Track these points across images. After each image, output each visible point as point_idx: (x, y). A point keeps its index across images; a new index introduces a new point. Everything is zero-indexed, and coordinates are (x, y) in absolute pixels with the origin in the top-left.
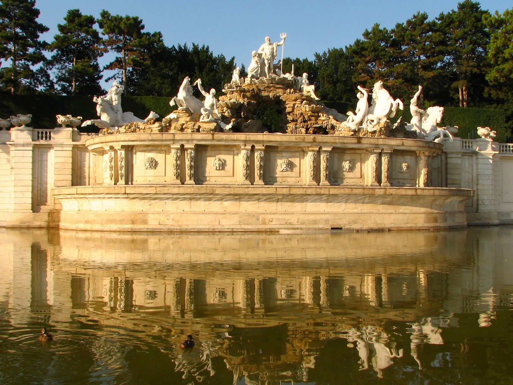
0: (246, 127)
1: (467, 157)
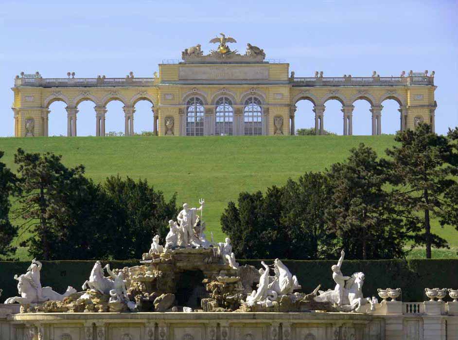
0: (158, 301)
1: (413, 322)
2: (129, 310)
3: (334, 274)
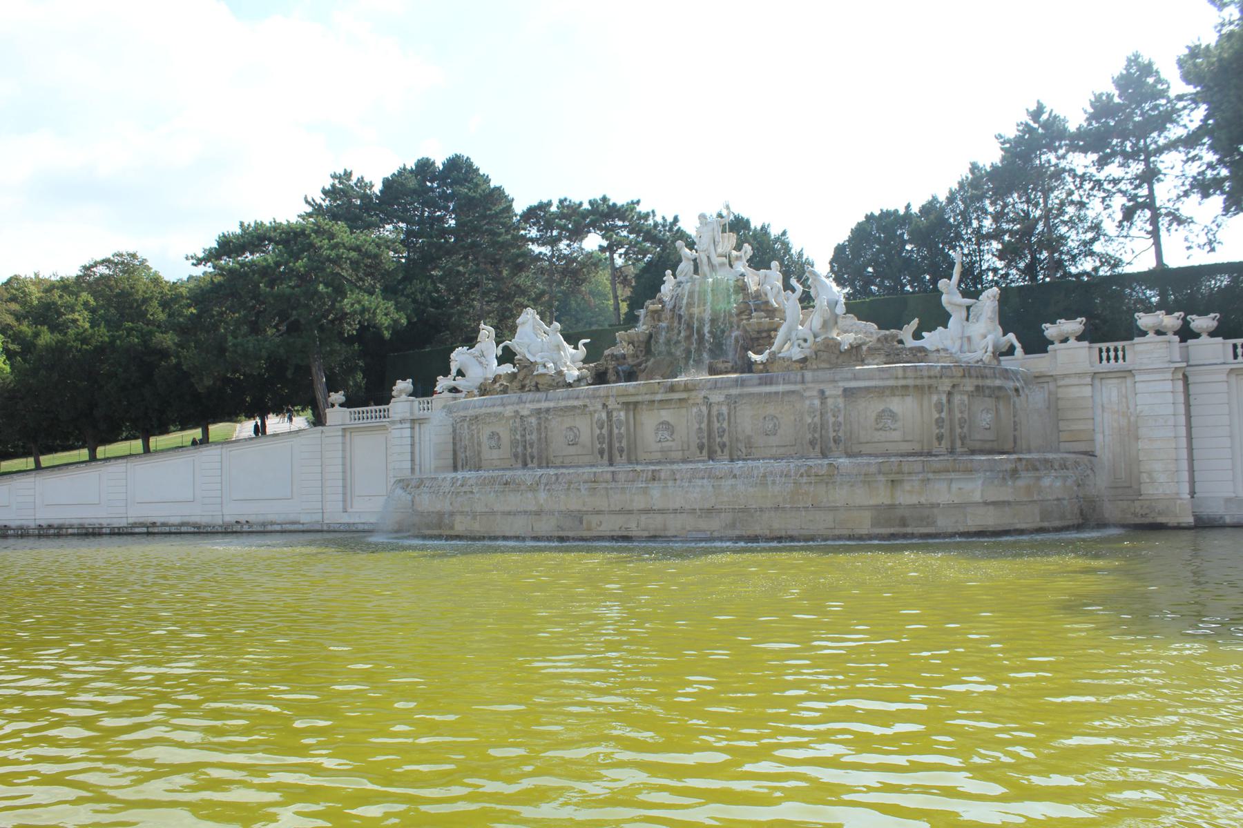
2: (570, 385)
3: (944, 298)
